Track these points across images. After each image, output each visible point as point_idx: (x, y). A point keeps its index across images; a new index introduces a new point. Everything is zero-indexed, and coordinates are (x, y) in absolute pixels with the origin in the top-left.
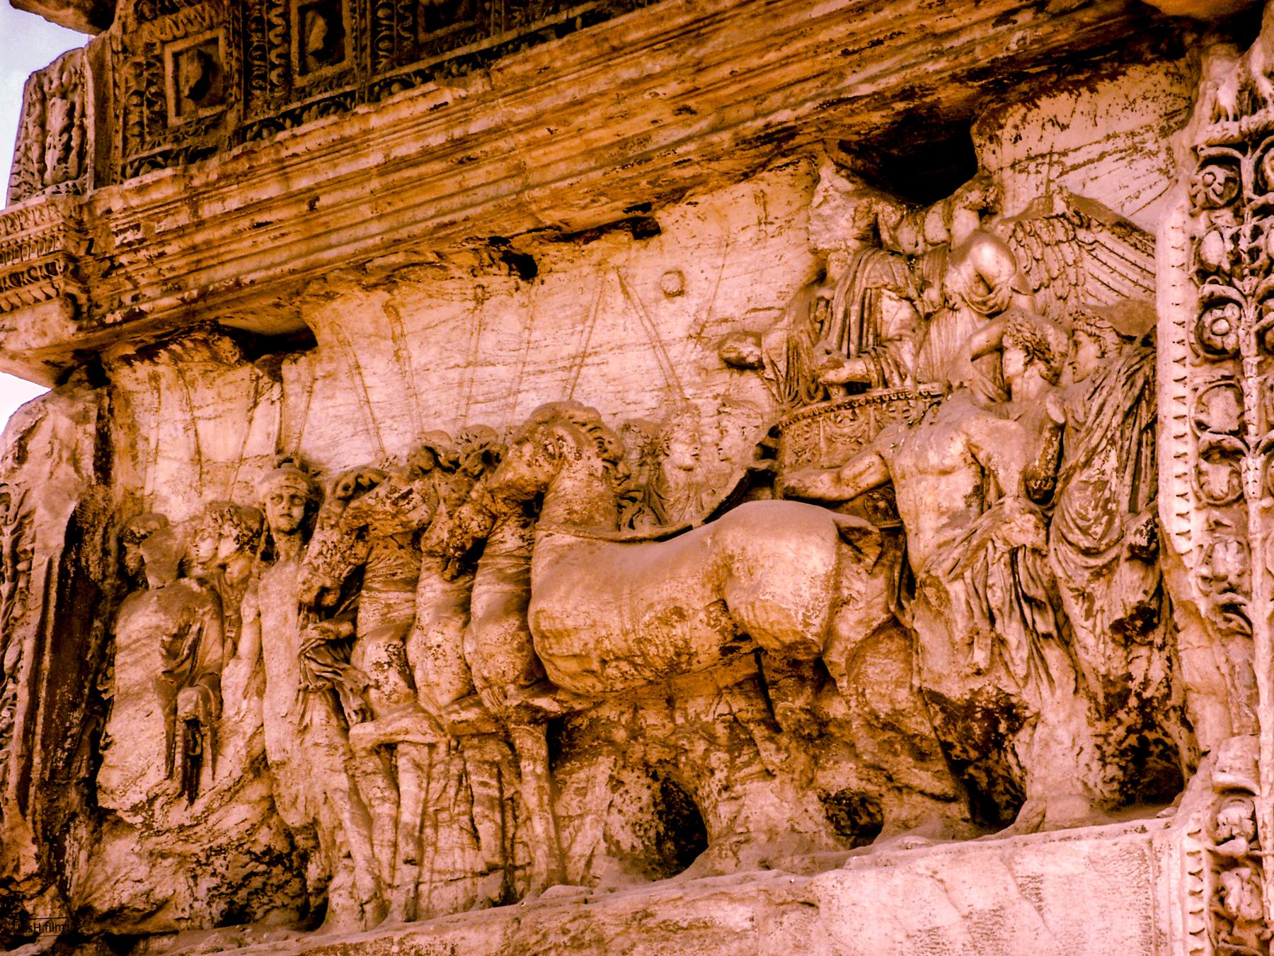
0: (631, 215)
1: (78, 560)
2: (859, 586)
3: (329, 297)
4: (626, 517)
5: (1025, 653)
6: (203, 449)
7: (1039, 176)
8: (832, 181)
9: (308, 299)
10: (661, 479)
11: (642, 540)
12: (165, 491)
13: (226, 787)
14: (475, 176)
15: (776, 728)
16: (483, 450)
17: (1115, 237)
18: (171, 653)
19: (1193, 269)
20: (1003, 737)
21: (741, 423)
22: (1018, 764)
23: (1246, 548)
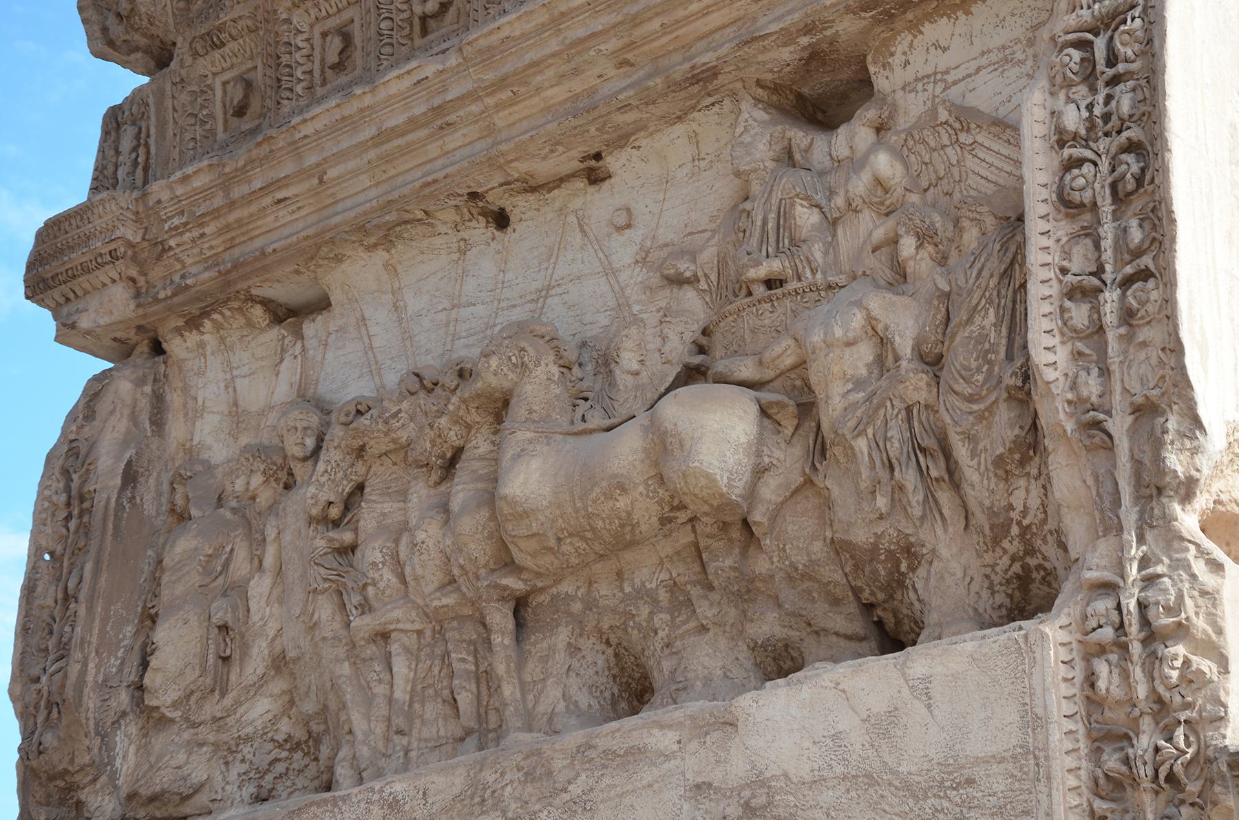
0: (586, 164)
1: (133, 498)
2: (778, 454)
3: (339, 259)
4: (578, 415)
5: (921, 497)
6: (240, 403)
7: (926, 93)
8: (753, 115)
9: (321, 262)
10: (612, 384)
11: (591, 432)
12: (209, 440)
13: (252, 683)
14: (454, 140)
15: (710, 587)
16: (458, 367)
17: (991, 136)
18: (206, 570)
19: (1055, 138)
20: (903, 574)
21: (680, 329)
22: (919, 600)
23: (1105, 372)
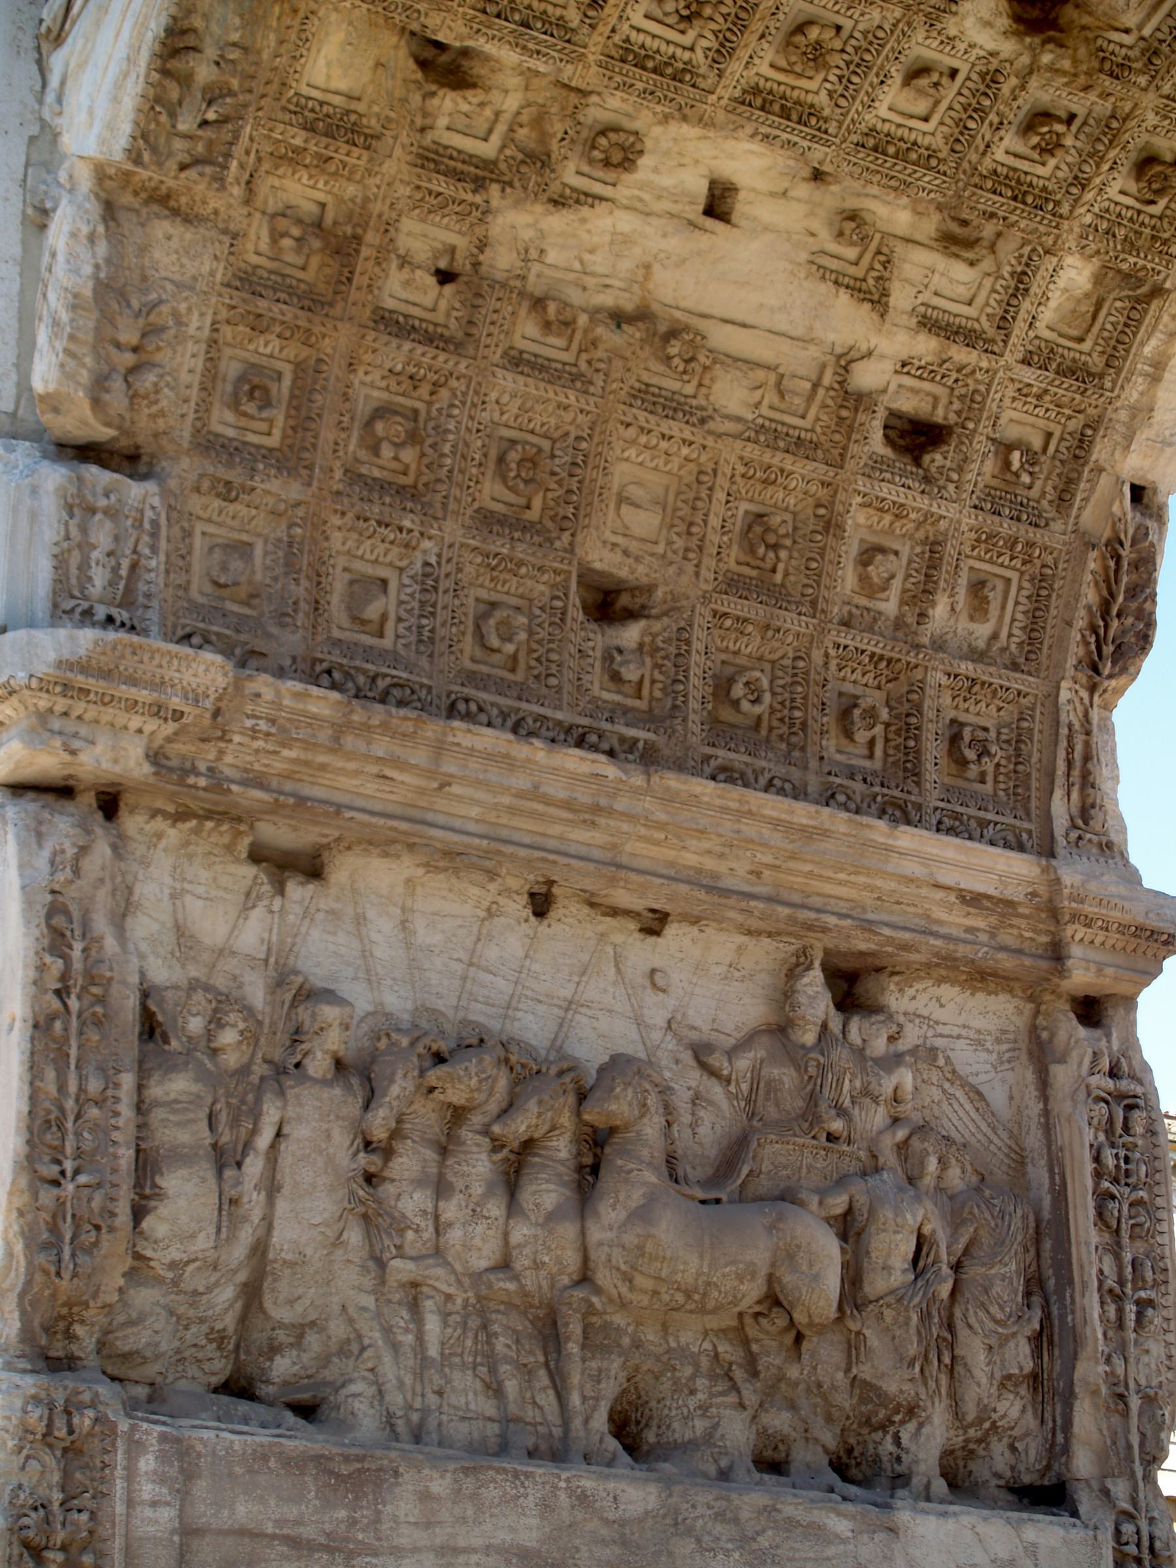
3: (386, 855)
